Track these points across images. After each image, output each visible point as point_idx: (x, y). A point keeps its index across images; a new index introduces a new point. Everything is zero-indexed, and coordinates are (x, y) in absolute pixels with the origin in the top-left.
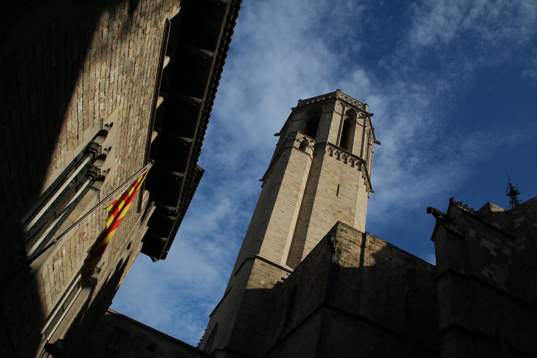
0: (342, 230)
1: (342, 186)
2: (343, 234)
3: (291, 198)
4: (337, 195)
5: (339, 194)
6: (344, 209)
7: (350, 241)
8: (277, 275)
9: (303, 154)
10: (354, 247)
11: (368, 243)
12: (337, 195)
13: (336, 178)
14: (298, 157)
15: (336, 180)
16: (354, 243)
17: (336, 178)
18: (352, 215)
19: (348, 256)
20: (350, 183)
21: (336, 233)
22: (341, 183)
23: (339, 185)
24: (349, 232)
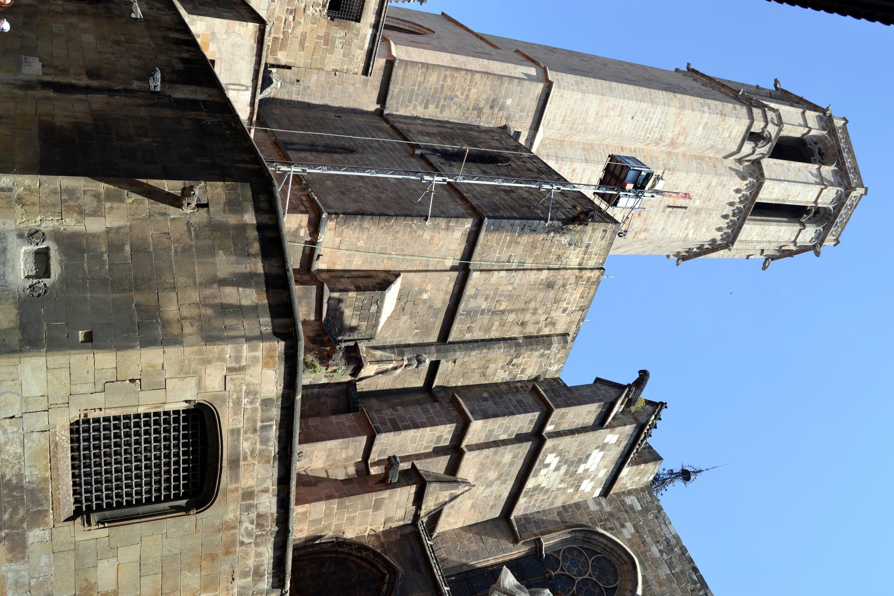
0: (605, 231)
1: (684, 213)
2: (599, 234)
3: (657, 130)
4: (669, 207)
5: (670, 209)
6: (645, 220)
7: (587, 247)
8: (524, 125)
9: (739, 140)
10: (578, 253)
11: (587, 274)
12: (669, 207)
13: (698, 203)
14: (734, 133)
15: (694, 202)
16: (585, 253)
17: (698, 203)
18: (636, 233)
19: (564, 245)
20: (691, 226)
21: (600, 222)
22: (690, 210)
23: (686, 208)
24: (603, 242)
